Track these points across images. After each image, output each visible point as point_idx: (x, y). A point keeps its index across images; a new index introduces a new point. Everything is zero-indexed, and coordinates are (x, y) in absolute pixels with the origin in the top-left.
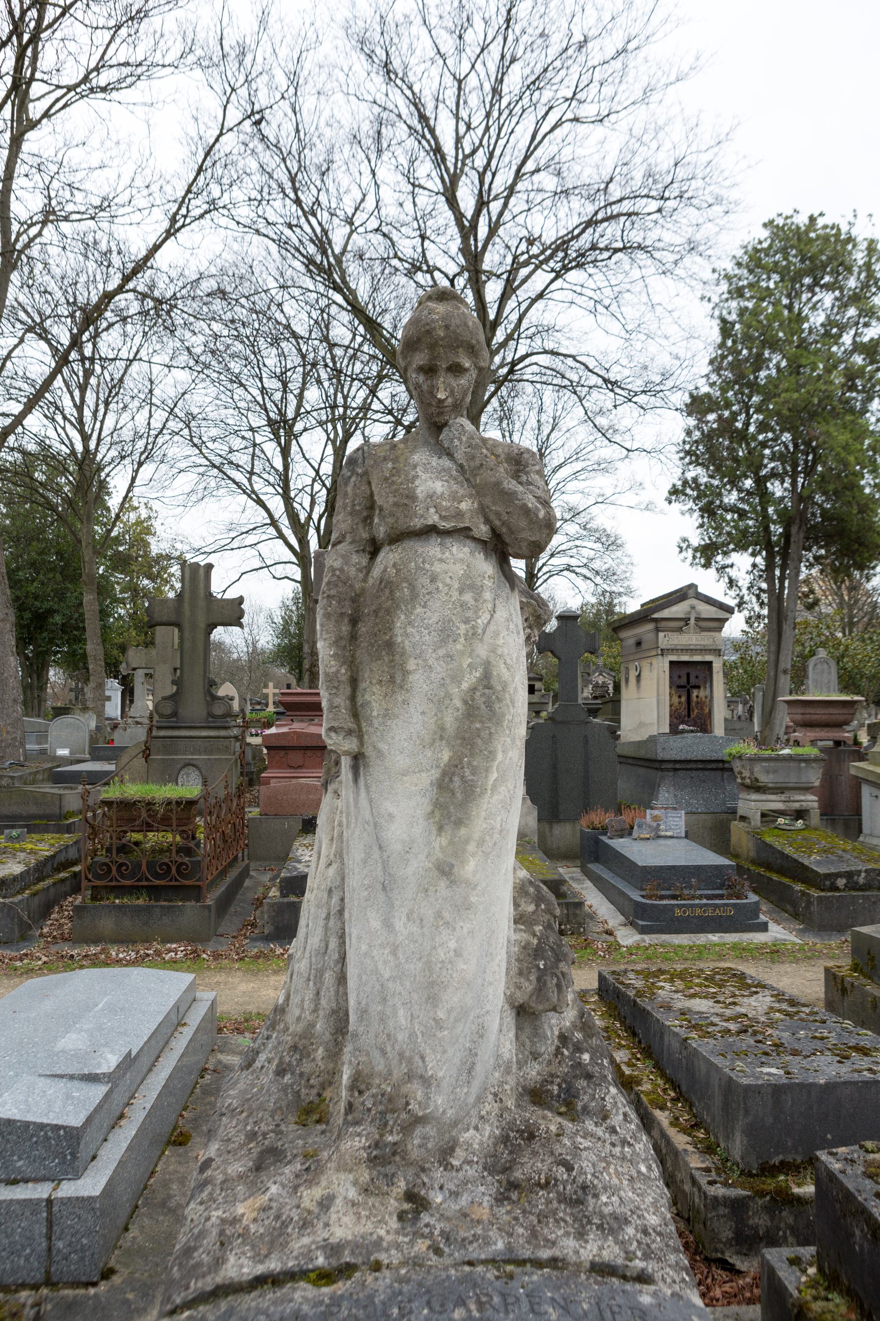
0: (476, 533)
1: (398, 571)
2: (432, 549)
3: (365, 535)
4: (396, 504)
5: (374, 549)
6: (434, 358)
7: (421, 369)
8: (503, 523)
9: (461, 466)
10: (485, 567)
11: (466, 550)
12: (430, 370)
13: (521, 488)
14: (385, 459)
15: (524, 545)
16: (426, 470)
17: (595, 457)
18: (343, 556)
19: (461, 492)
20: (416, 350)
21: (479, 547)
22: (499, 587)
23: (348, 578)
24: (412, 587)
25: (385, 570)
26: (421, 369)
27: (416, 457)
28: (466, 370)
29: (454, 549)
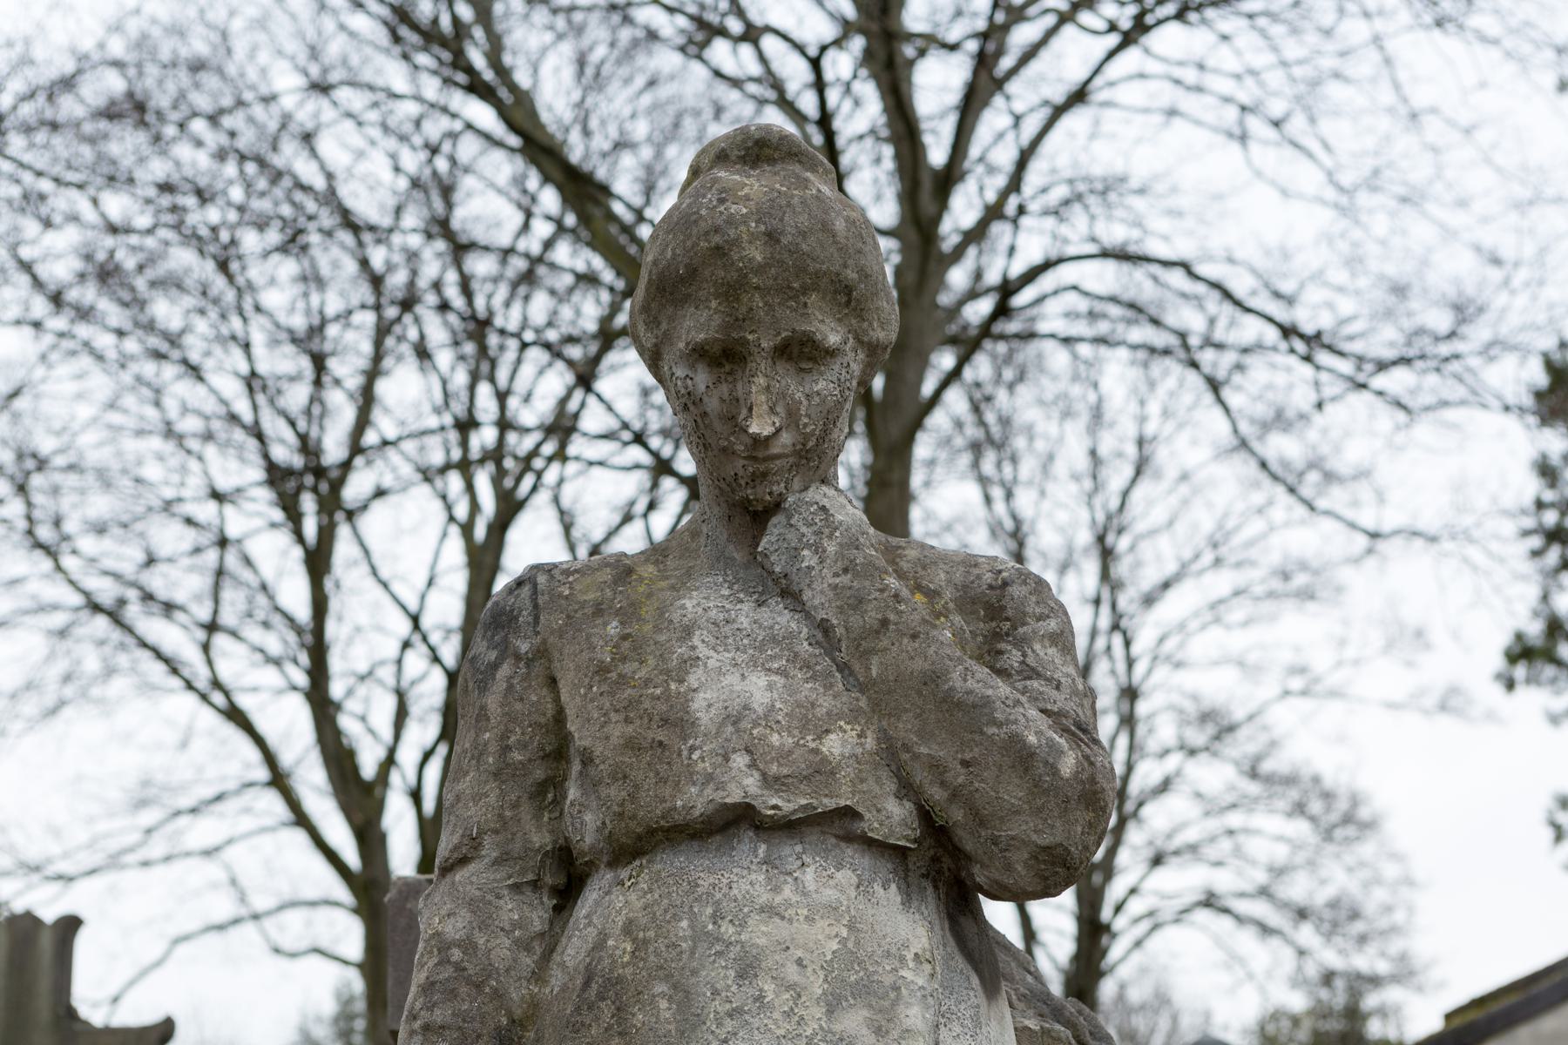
0: (873, 826)
1: (640, 946)
2: (742, 876)
3: (541, 839)
4: (631, 745)
5: (566, 879)
6: (737, 322)
7: (699, 354)
8: (955, 795)
9: (825, 627)
10: (906, 928)
11: (845, 877)
12: (725, 357)
13: (1002, 689)
14: (599, 610)
15: (1019, 858)
16: (720, 643)
17: (1273, 554)
18: (472, 905)
19: (826, 703)
20: (686, 299)
21: (885, 866)
22: (948, 988)
23: (489, 971)
24: (683, 996)
25: (600, 945)
26: (699, 354)
27: (690, 604)
28: (832, 353)
29: (809, 876)
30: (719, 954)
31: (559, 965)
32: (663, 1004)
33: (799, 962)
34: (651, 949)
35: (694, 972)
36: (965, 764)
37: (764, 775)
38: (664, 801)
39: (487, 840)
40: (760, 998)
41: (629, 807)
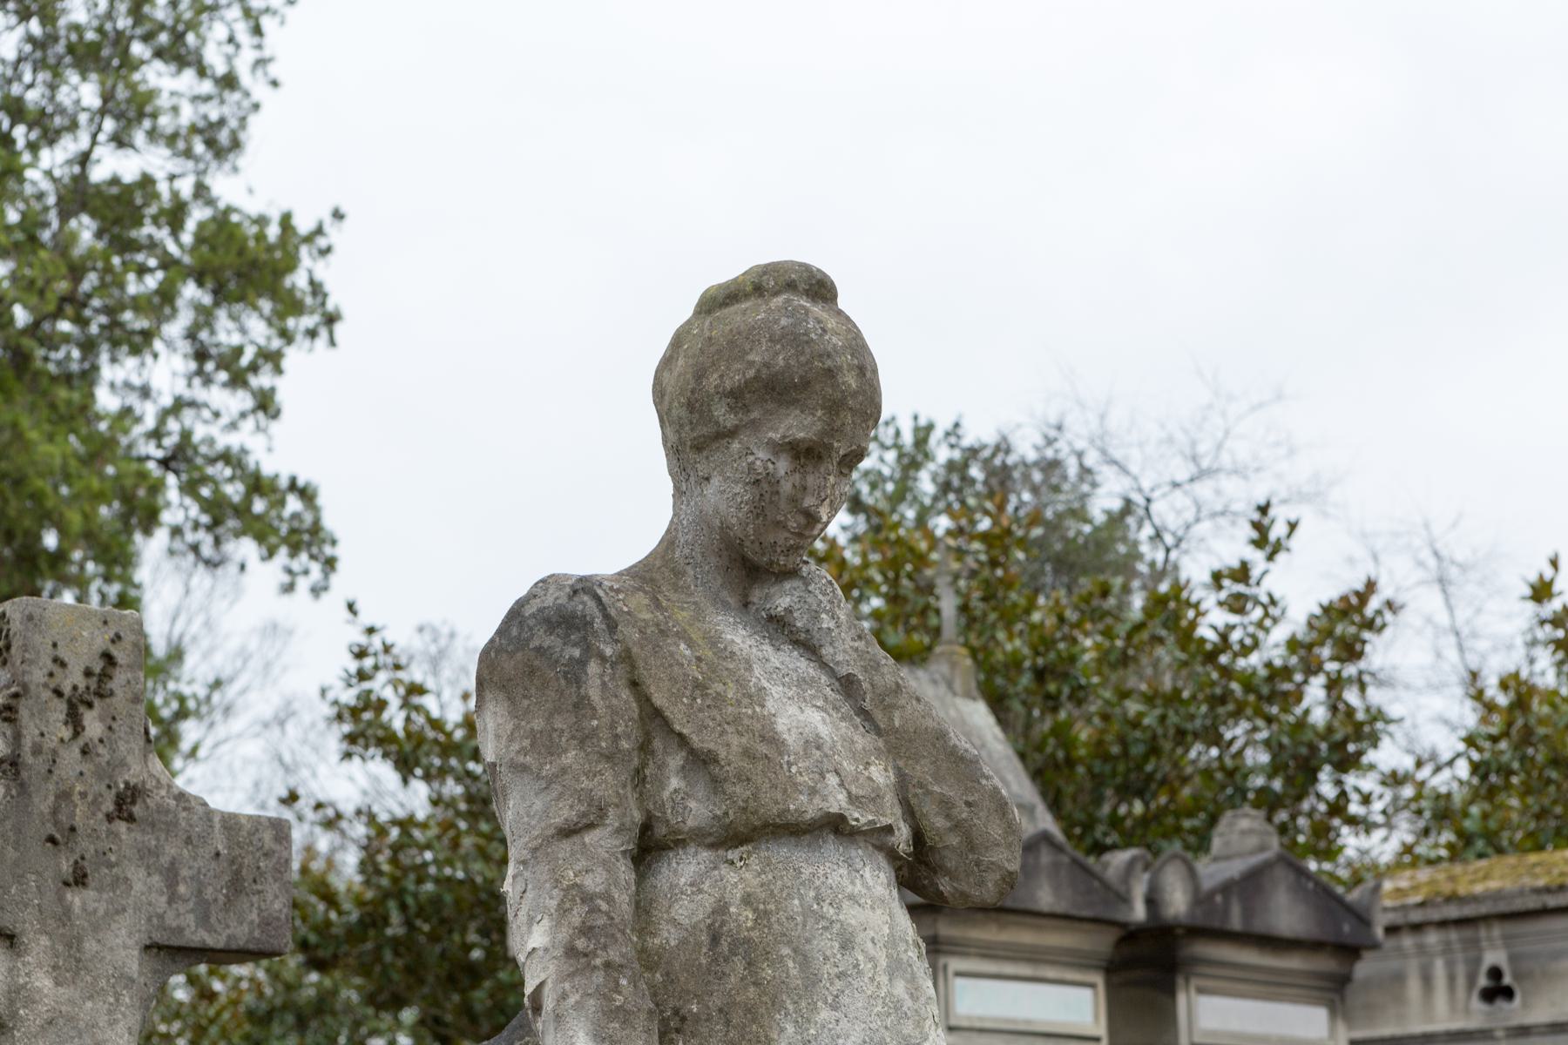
1: (762, 916)
4: (747, 753)
5: (649, 848)
6: (832, 431)
20: (794, 402)
24: (804, 961)
30: (825, 928)
31: (668, 922)
32: (791, 964)
33: (873, 940)
34: (773, 919)
35: (808, 941)
36: (968, 804)
37: (849, 793)
38: (777, 803)
39: (611, 812)
40: (856, 966)
41: (752, 804)
